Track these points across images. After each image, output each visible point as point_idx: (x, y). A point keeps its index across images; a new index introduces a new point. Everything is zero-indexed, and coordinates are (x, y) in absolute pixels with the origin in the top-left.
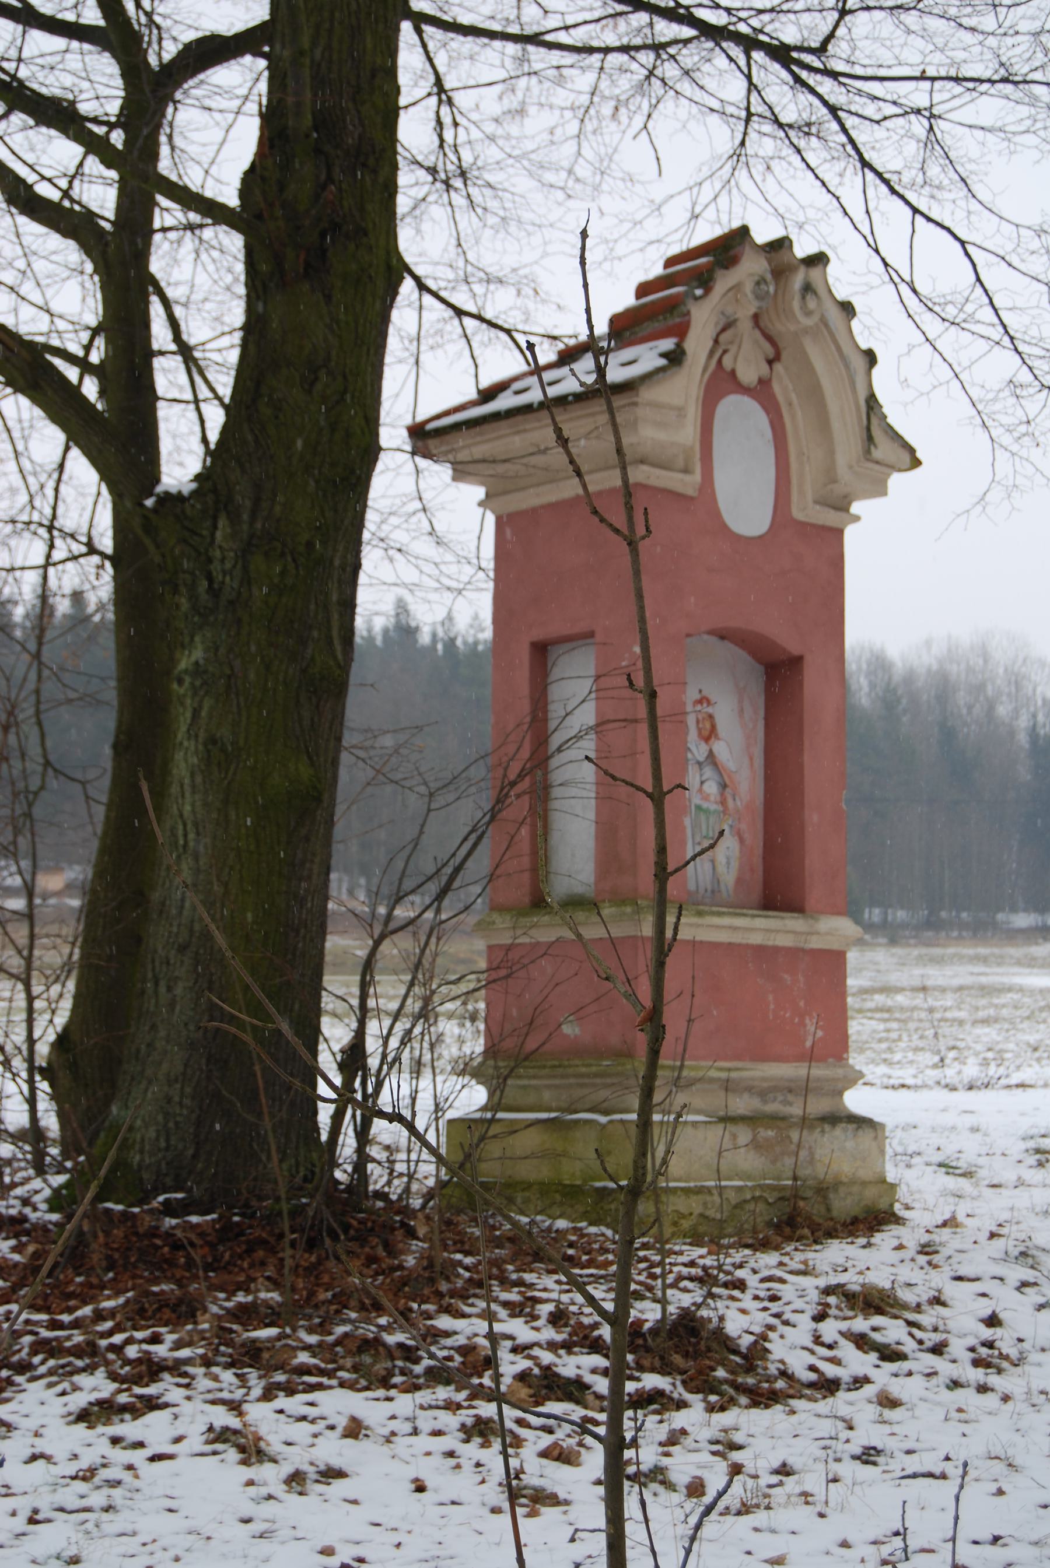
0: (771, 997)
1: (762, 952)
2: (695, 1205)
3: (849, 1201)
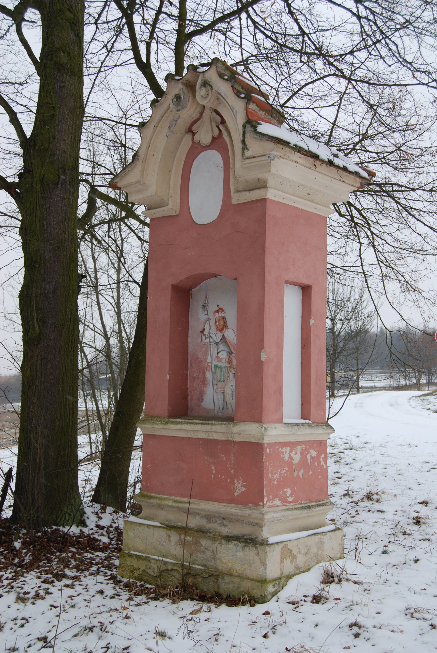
0: (213, 467)
1: (208, 442)
2: (142, 565)
3: (231, 586)
